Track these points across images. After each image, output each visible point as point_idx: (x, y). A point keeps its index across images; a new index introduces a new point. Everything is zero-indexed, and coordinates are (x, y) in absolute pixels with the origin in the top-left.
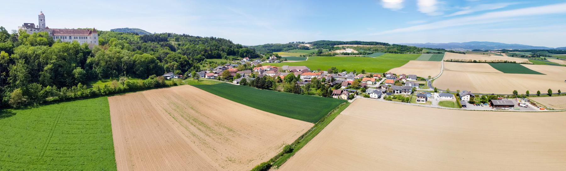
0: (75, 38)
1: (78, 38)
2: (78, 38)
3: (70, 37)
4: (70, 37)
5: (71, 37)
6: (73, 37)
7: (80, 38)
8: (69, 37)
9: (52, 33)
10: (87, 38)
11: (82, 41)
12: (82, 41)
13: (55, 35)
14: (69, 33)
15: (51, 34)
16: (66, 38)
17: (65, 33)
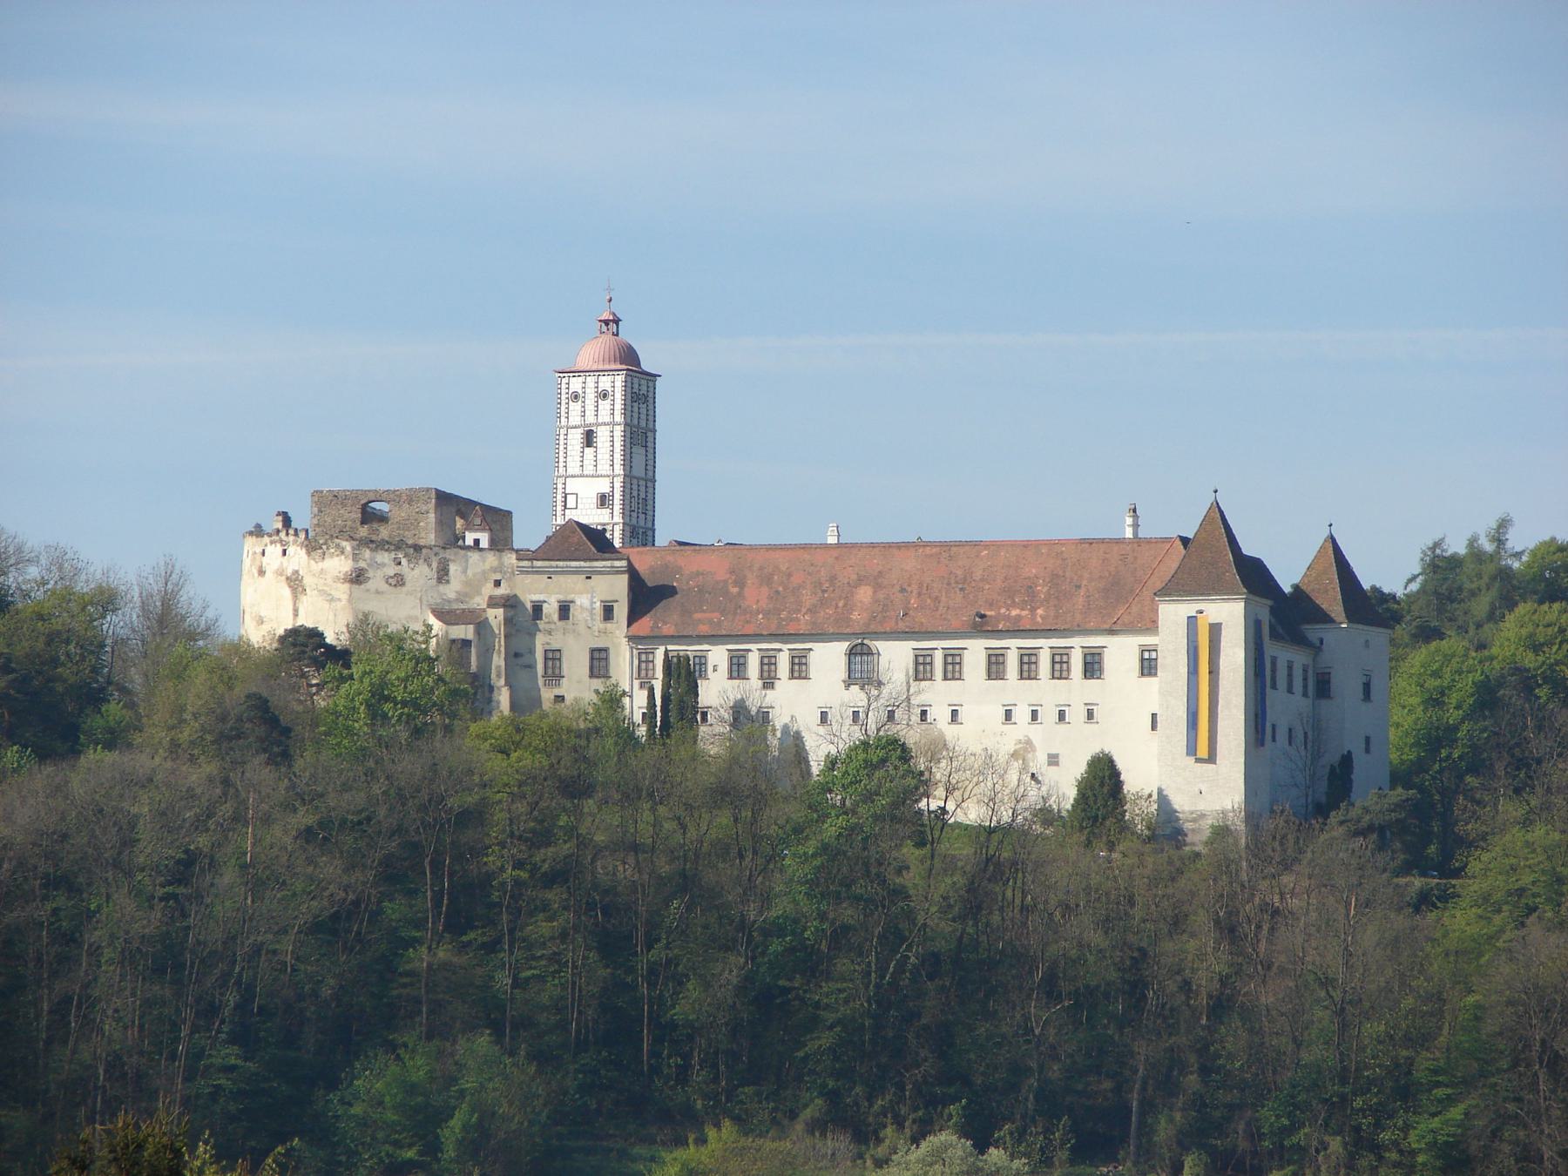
10: (1093, 667)
11: (1022, 714)
12: (1022, 714)
15: (608, 612)
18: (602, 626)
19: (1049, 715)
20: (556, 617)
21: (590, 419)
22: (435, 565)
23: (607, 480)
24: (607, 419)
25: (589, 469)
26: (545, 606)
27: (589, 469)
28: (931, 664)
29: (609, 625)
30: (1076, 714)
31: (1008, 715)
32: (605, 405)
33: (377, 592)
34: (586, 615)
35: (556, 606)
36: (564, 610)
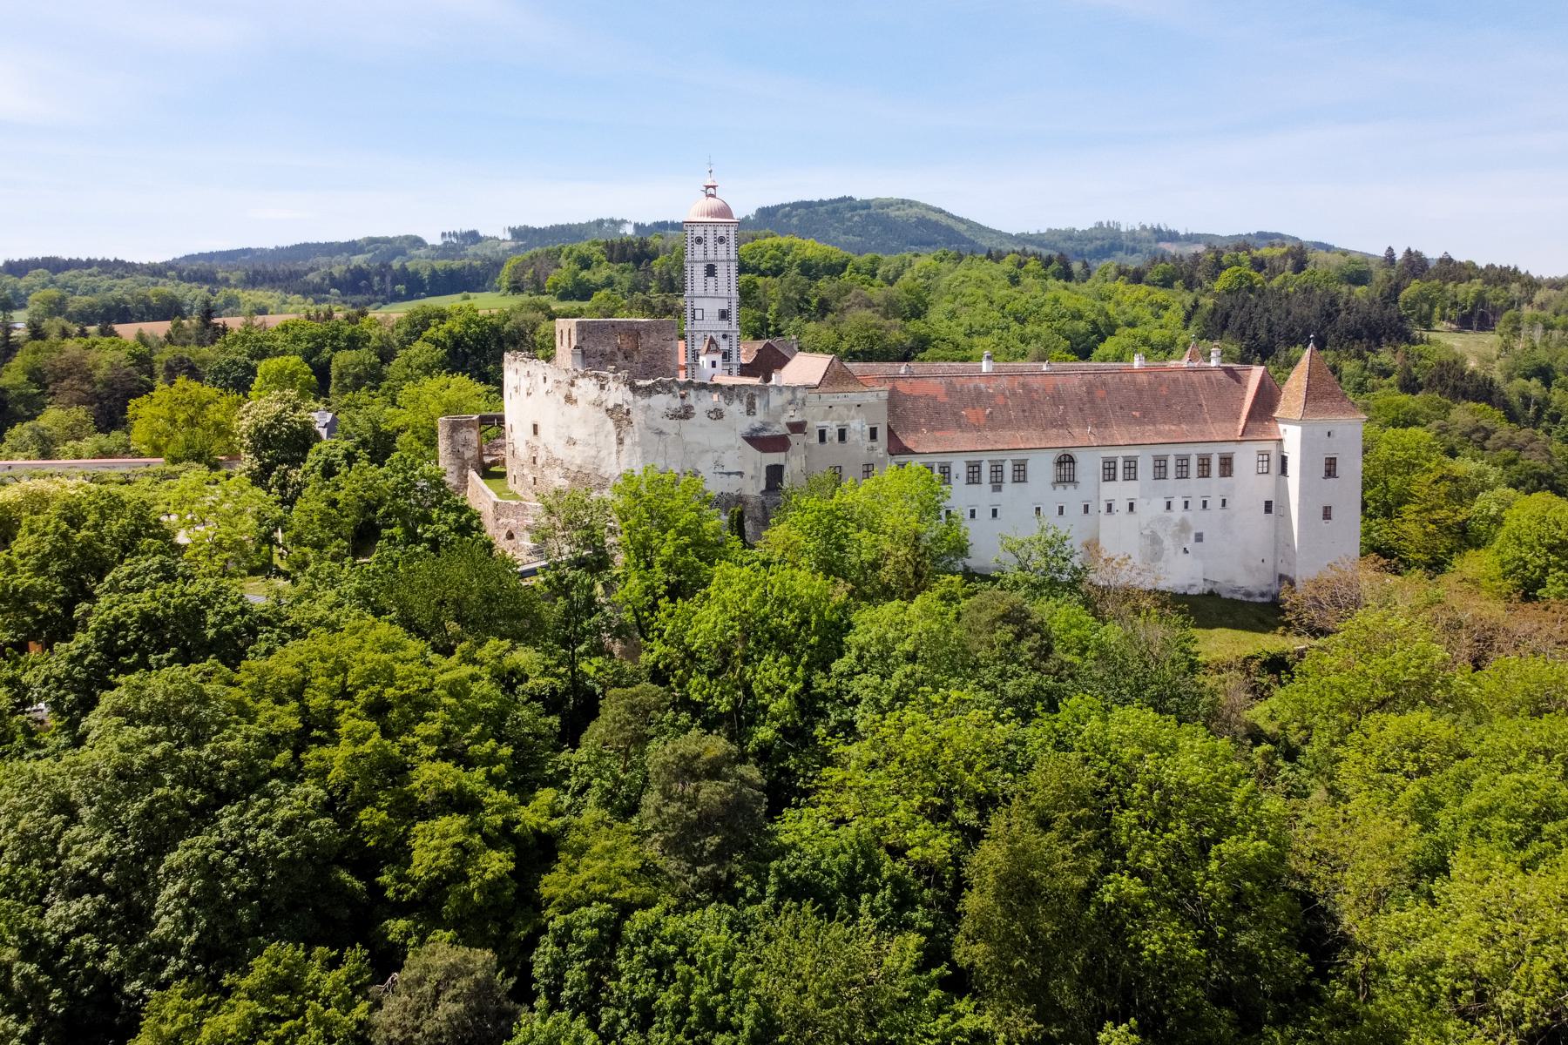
0: (1109, 473)
1: (1145, 467)
2: (1145, 467)
3: (1066, 461)
4: (1066, 461)
5: (1072, 460)
6: (1088, 464)
7: (1183, 474)
8: (1052, 456)
9: (882, 434)
10: (1227, 465)
11: (1178, 504)
12: (1178, 504)
13: (909, 444)
14: (1053, 424)
15: (873, 434)
16: (1020, 473)
17: (1008, 424)
18: (870, 444)
19: (1196, 504)
20: (836, 439)
21: (711, 256)
22: (745, 400)
23: (726, 301)
24: (725, 257)
25: (711, 291)
26: (828, 430)
27: (711, 291)
28: (1114, 468)
29: (874, 444)
30: (1214, 503)
31: (1169, 506)
32: (722, 248)
33: (701, 426)
34: (858, 437)
35: (836, 430)
36: (842, 435)
